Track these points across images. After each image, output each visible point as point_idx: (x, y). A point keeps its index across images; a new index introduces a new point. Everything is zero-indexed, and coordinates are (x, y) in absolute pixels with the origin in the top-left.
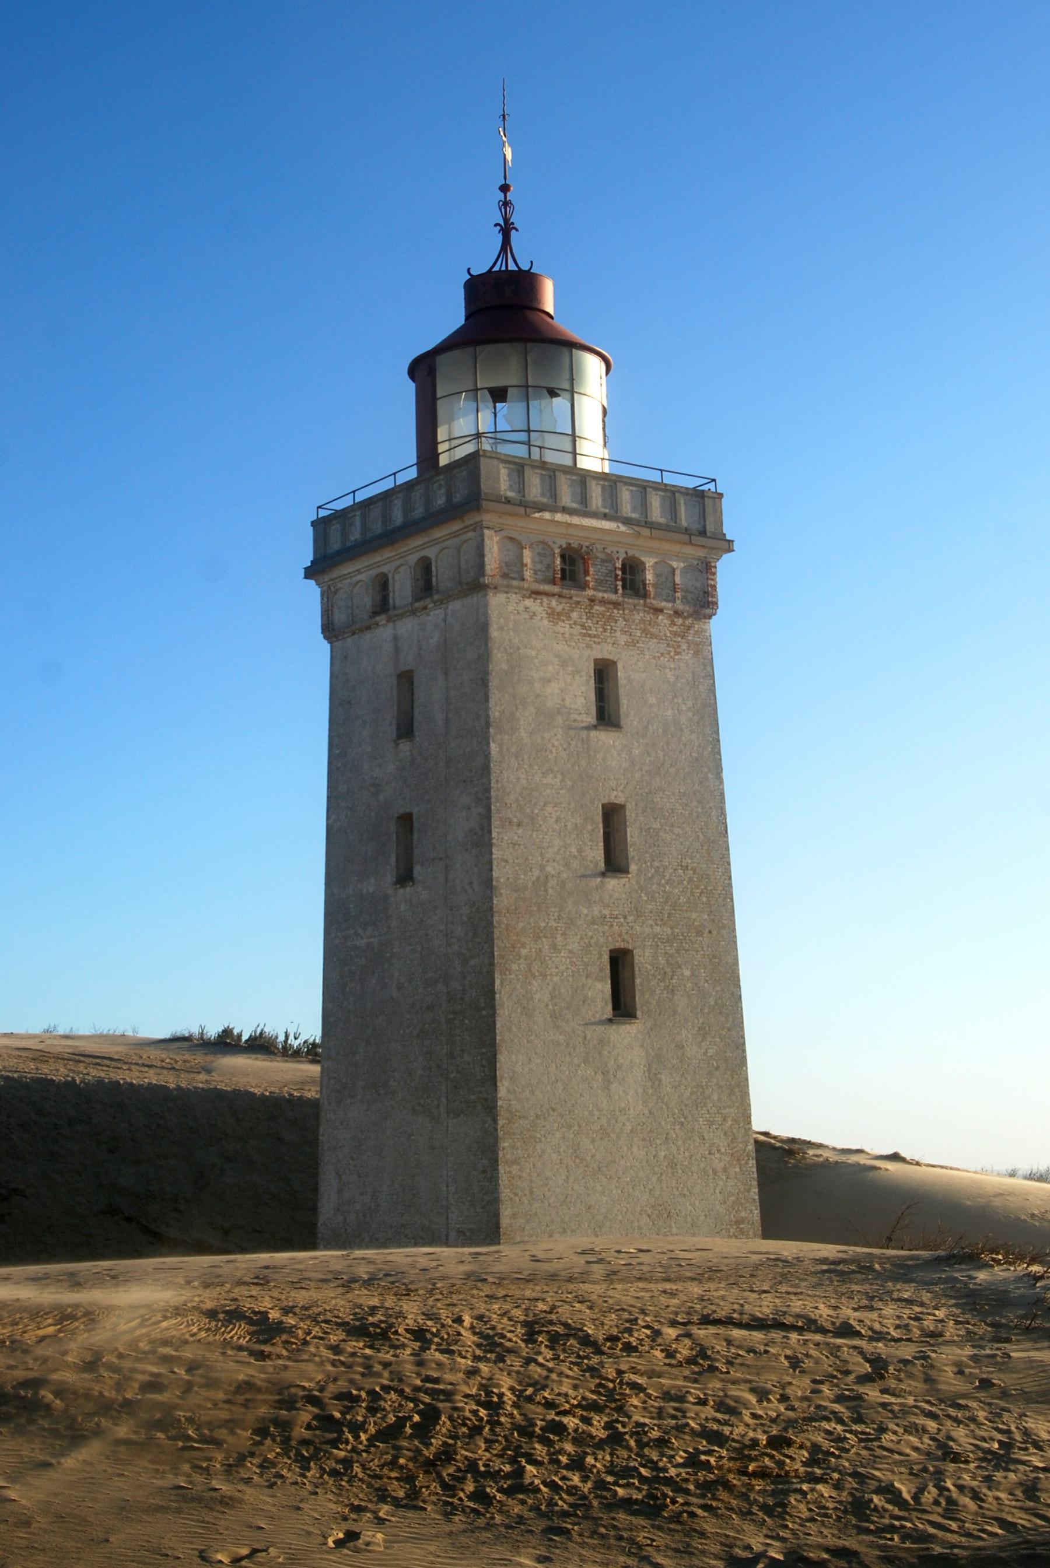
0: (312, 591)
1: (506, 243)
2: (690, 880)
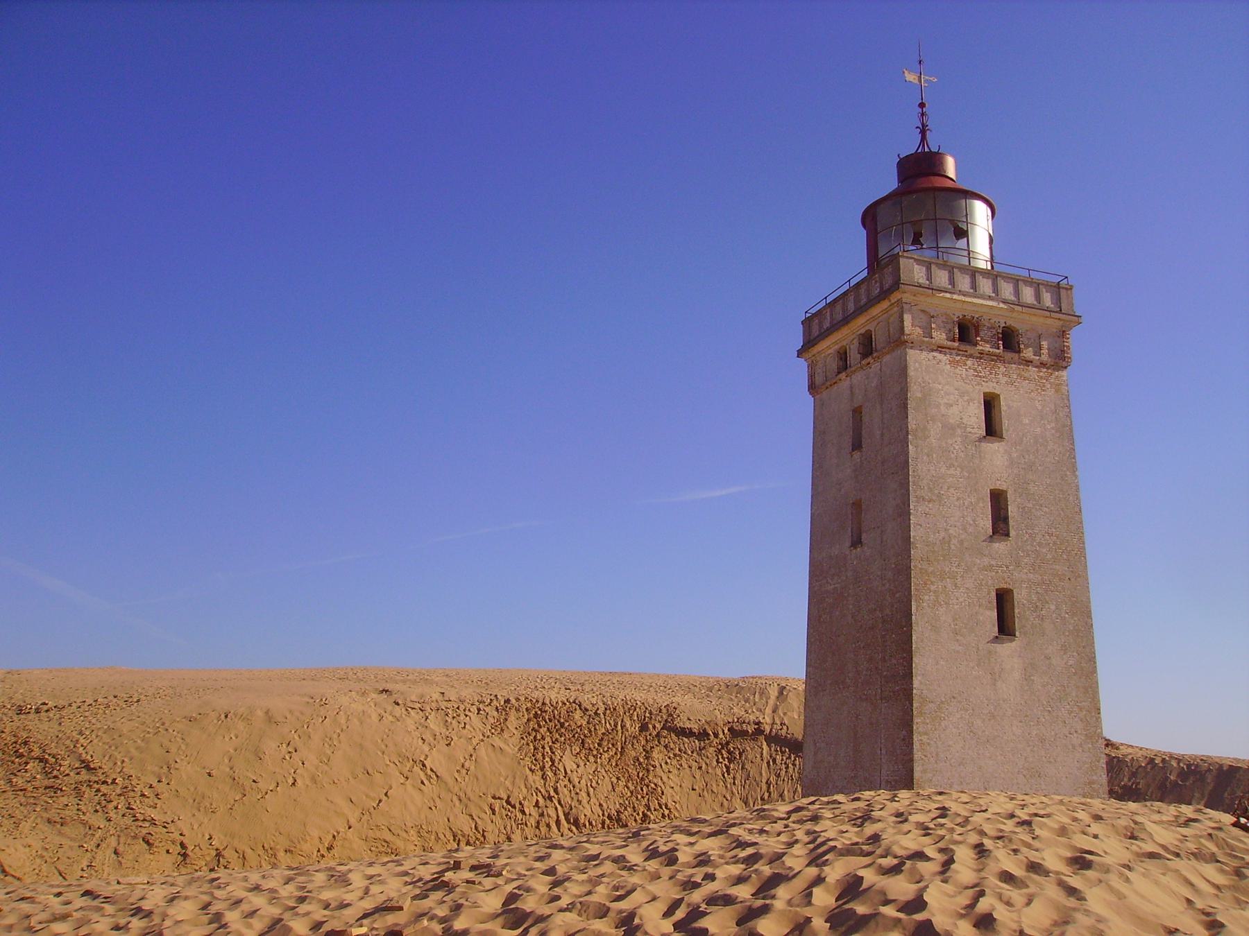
2: (1055, 543)
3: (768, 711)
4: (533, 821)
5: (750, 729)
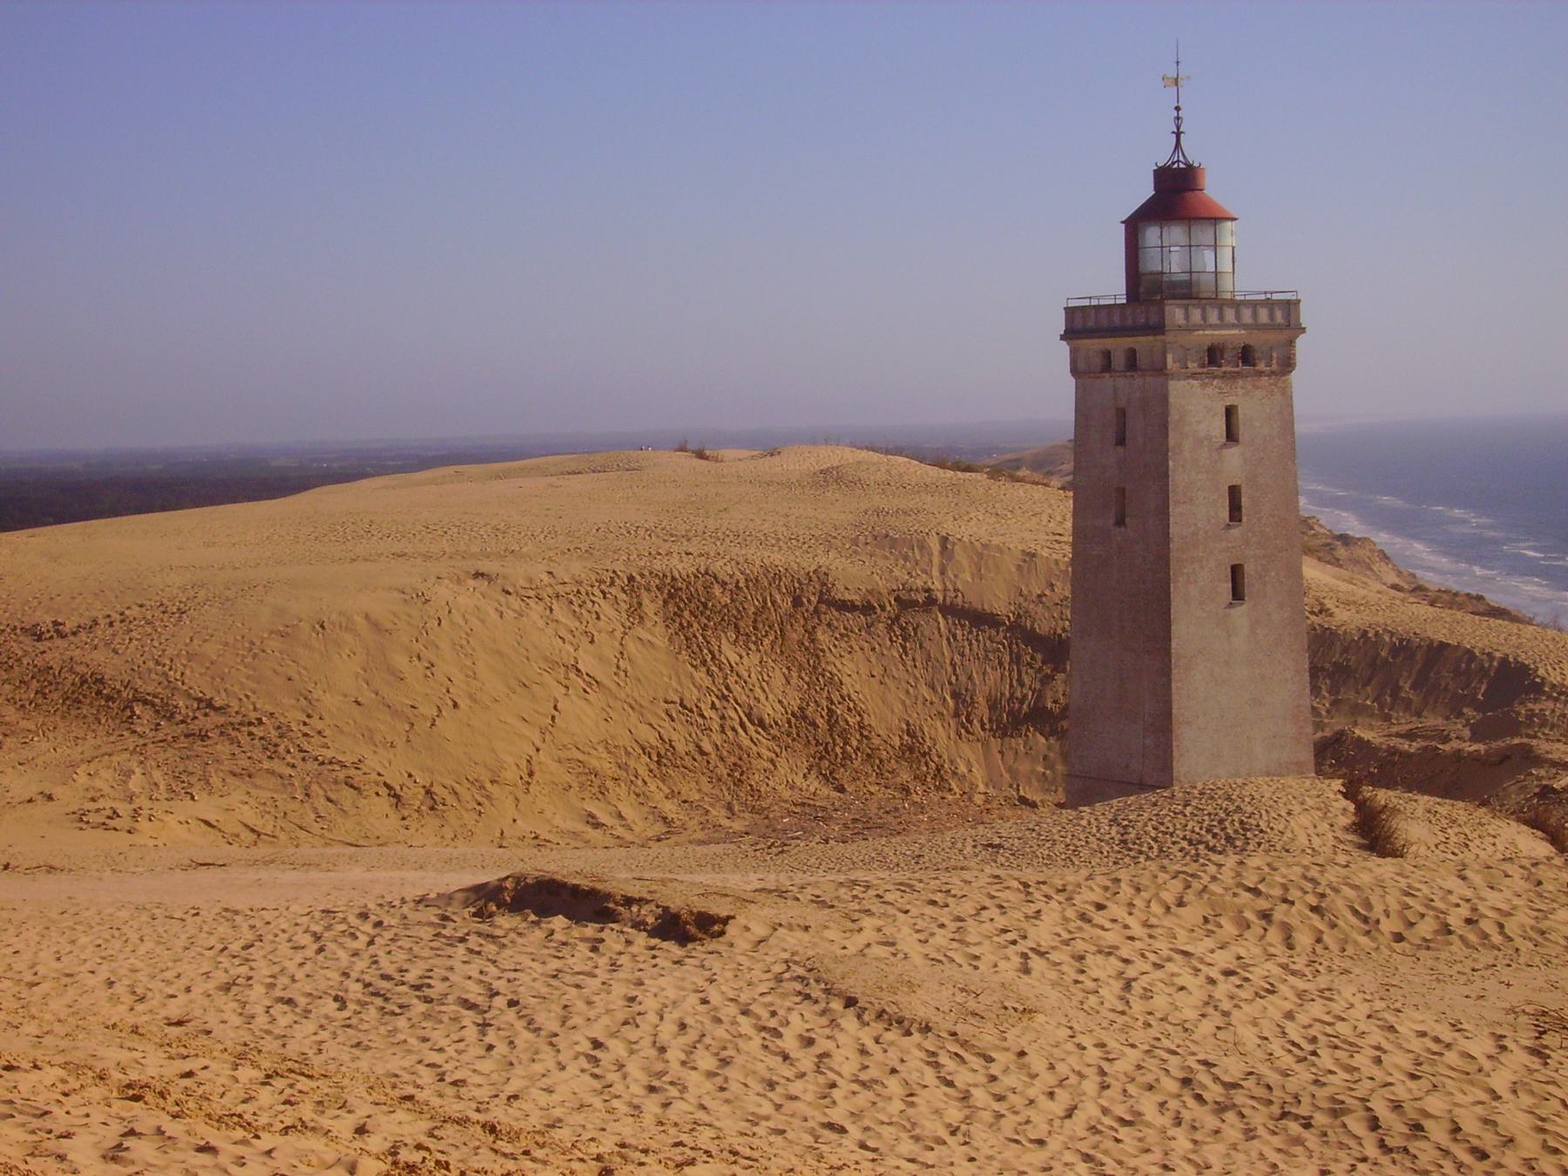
0: (1065, 348)
3: (936, 573)
4: (715, 726)
5: (921, 598)
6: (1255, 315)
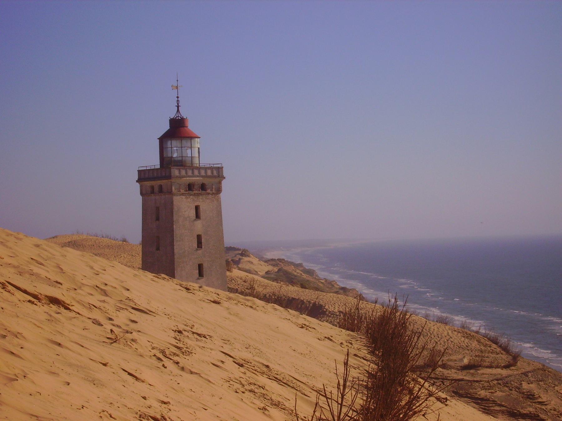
0: (138, 185)
1: (178, 110)
6: (206, 172)
